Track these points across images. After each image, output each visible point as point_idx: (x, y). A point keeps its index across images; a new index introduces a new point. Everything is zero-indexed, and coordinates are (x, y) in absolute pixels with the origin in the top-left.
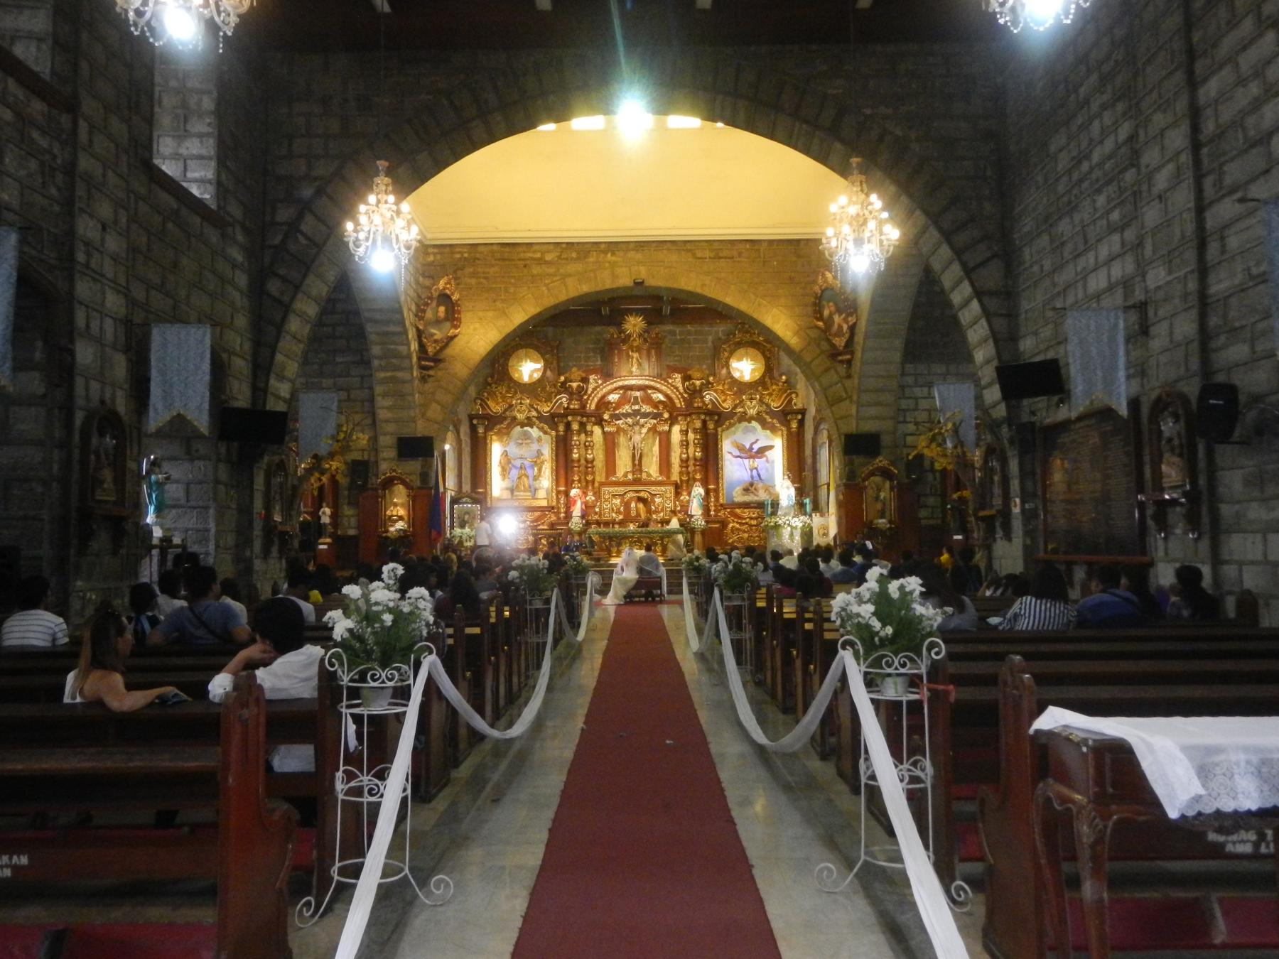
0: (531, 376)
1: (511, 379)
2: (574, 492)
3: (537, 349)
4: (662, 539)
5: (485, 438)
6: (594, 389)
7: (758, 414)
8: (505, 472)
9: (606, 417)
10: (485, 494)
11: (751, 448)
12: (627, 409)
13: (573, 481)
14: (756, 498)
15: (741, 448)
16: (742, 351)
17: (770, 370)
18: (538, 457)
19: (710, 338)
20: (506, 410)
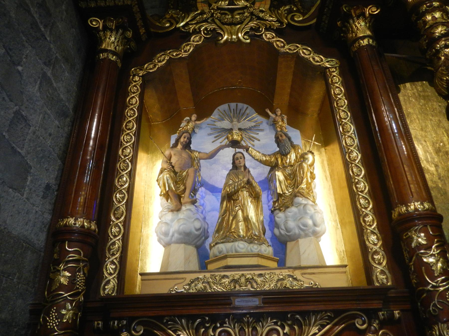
8: (180, 191)
10: (95, 246)
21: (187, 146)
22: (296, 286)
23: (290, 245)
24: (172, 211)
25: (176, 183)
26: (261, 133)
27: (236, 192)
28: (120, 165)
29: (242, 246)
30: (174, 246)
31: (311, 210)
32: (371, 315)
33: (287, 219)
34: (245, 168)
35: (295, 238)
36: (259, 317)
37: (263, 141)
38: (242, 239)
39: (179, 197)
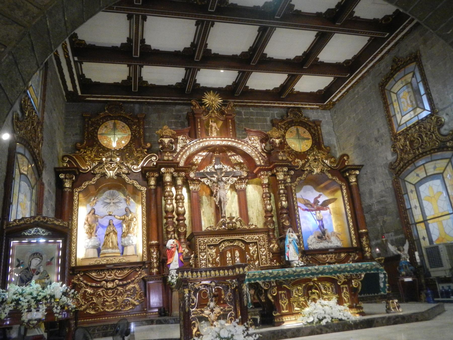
0: (118, 143)
1: (100, 145)
2: (170, 243)
3: (125, 120)
4: (348, 282)
5: (72, 195)
6: (183, 148)
7: (322, 171)
9: (192, 175)
11: (316, 201)
12: (209, 168)
13: (168, 233)
14: (330, 245)
15: (307, 203)
16: (293, 129)
17: (317, 143)
18: (127, 215)
19: (268, 119)
20: (95, 167)
21: (94, 213)
22: (124, 261)
23: (125, 248)
24: (89, 238)
25: (90, 229)
26: (121, 204)
27: (109, 233)
28: (74, 227)
29: (110, 250)
30: (90, 249)
31: (132, 238)
32: (140, 267)
33: (125, 241)
34: (113, 224)
35: (126, 246)
36: (113, 269)
37: (122, 207)
38: (110, 248)
39: (91, 233)
